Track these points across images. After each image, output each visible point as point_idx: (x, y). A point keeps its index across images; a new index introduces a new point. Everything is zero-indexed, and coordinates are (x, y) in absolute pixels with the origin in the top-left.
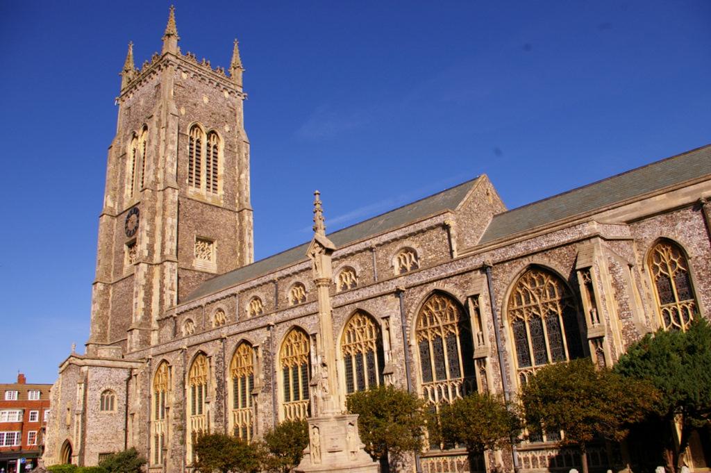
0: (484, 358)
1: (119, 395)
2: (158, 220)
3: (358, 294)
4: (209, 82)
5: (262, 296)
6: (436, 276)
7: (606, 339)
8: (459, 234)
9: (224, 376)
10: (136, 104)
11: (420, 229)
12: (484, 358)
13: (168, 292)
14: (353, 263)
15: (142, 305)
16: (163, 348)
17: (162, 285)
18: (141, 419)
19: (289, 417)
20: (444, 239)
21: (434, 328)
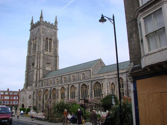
1: (32, 96)
2: (39, 59)
13: (41, 75)
14: (75, 75)
15: (35, 78)
16: (40, 88)
17: (40, 74)
18: (36, 101)
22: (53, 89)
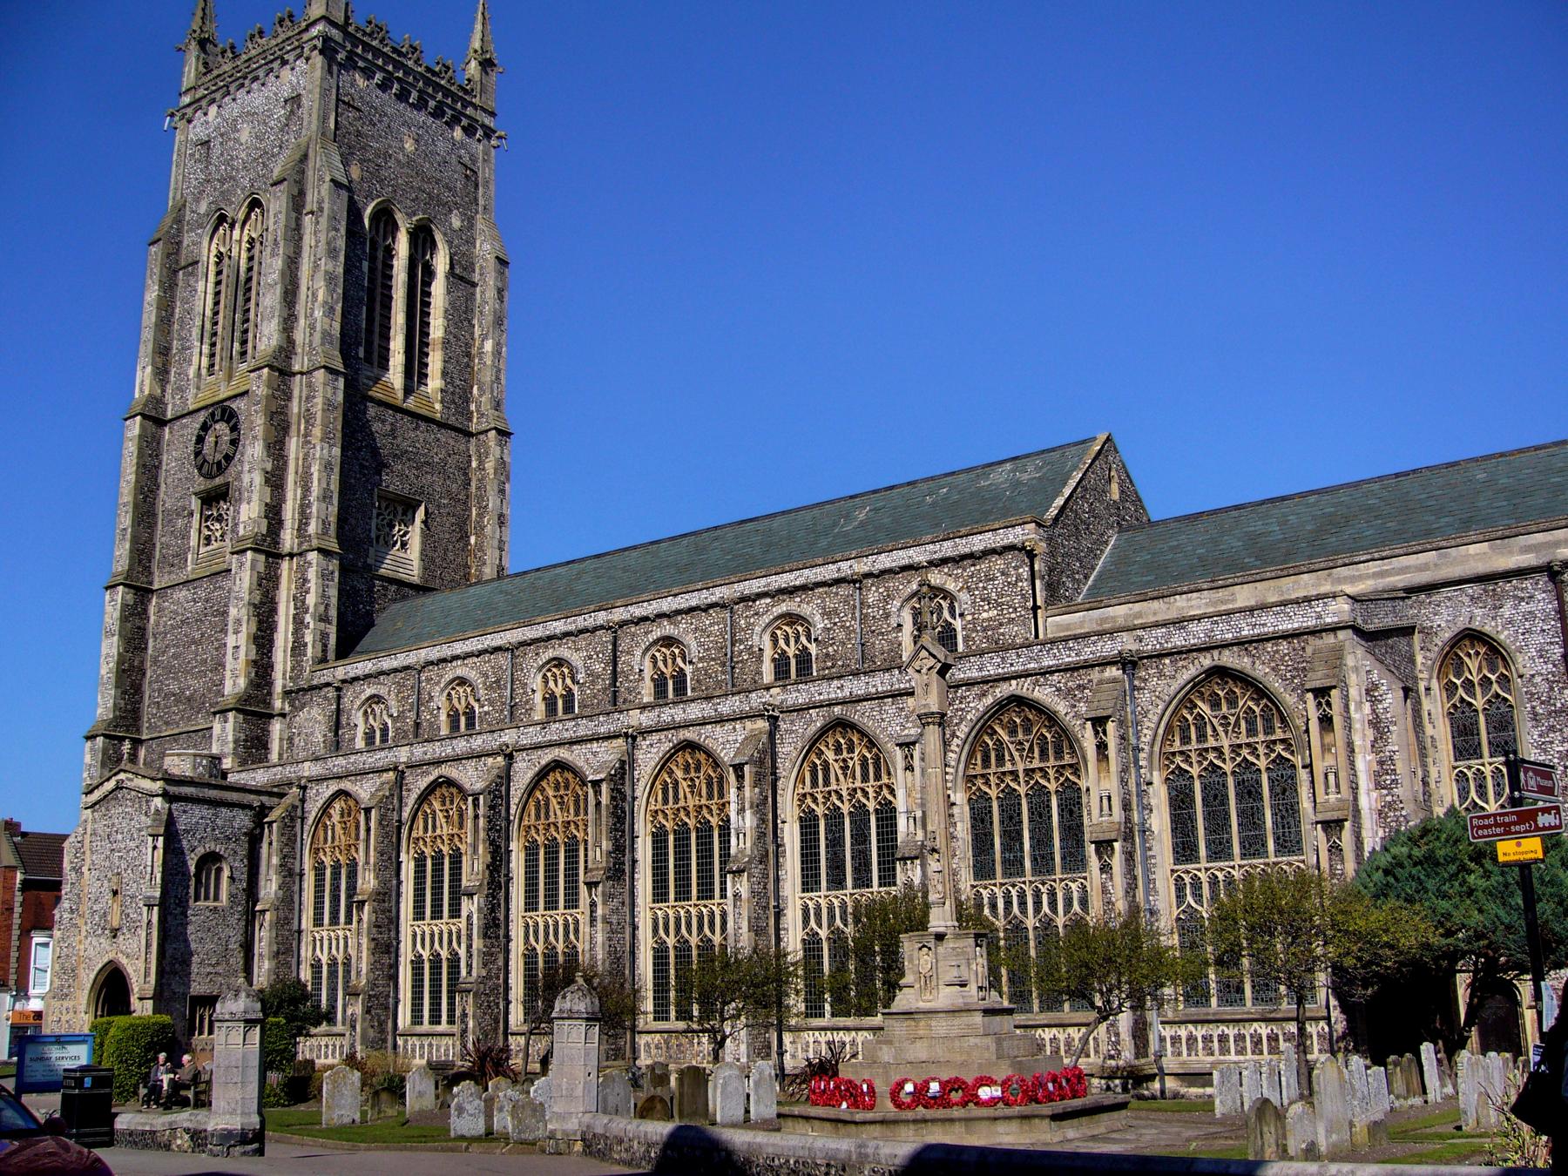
0: (1110, 842)
2: (293, 446)
3: (841, 688)
5: (576, 659)
6: (1018, 668)
7: (1347, 824)
8: (1051, 570)
9: (508, 840)
10: (228, 132)
11: (967, 550)
12: (1110, 842)
14: (807, 608)
19: (686, 935)
20: (1019, 579)
21: (1004, 773)
22: (543, 774)
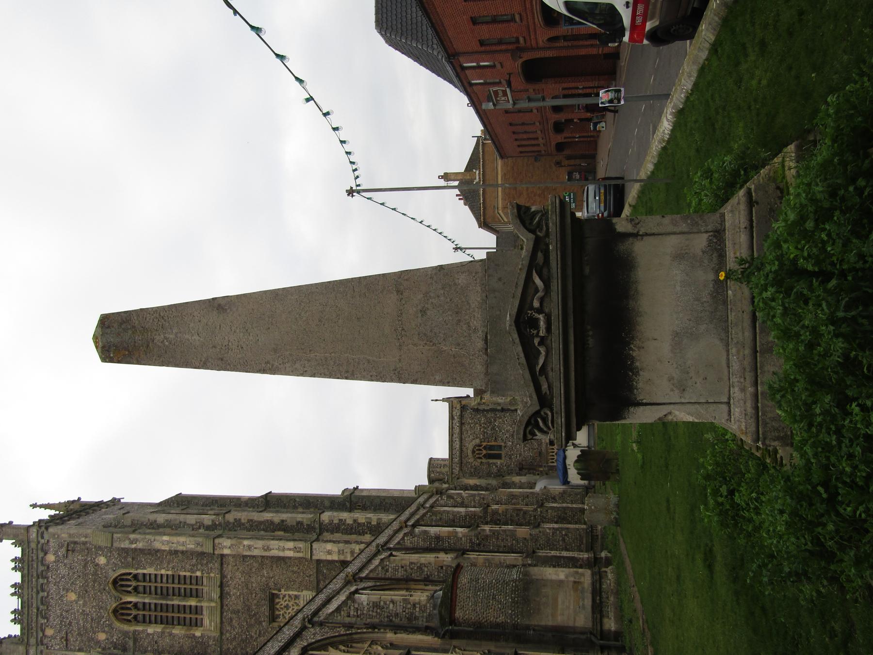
4: (43, 590)
